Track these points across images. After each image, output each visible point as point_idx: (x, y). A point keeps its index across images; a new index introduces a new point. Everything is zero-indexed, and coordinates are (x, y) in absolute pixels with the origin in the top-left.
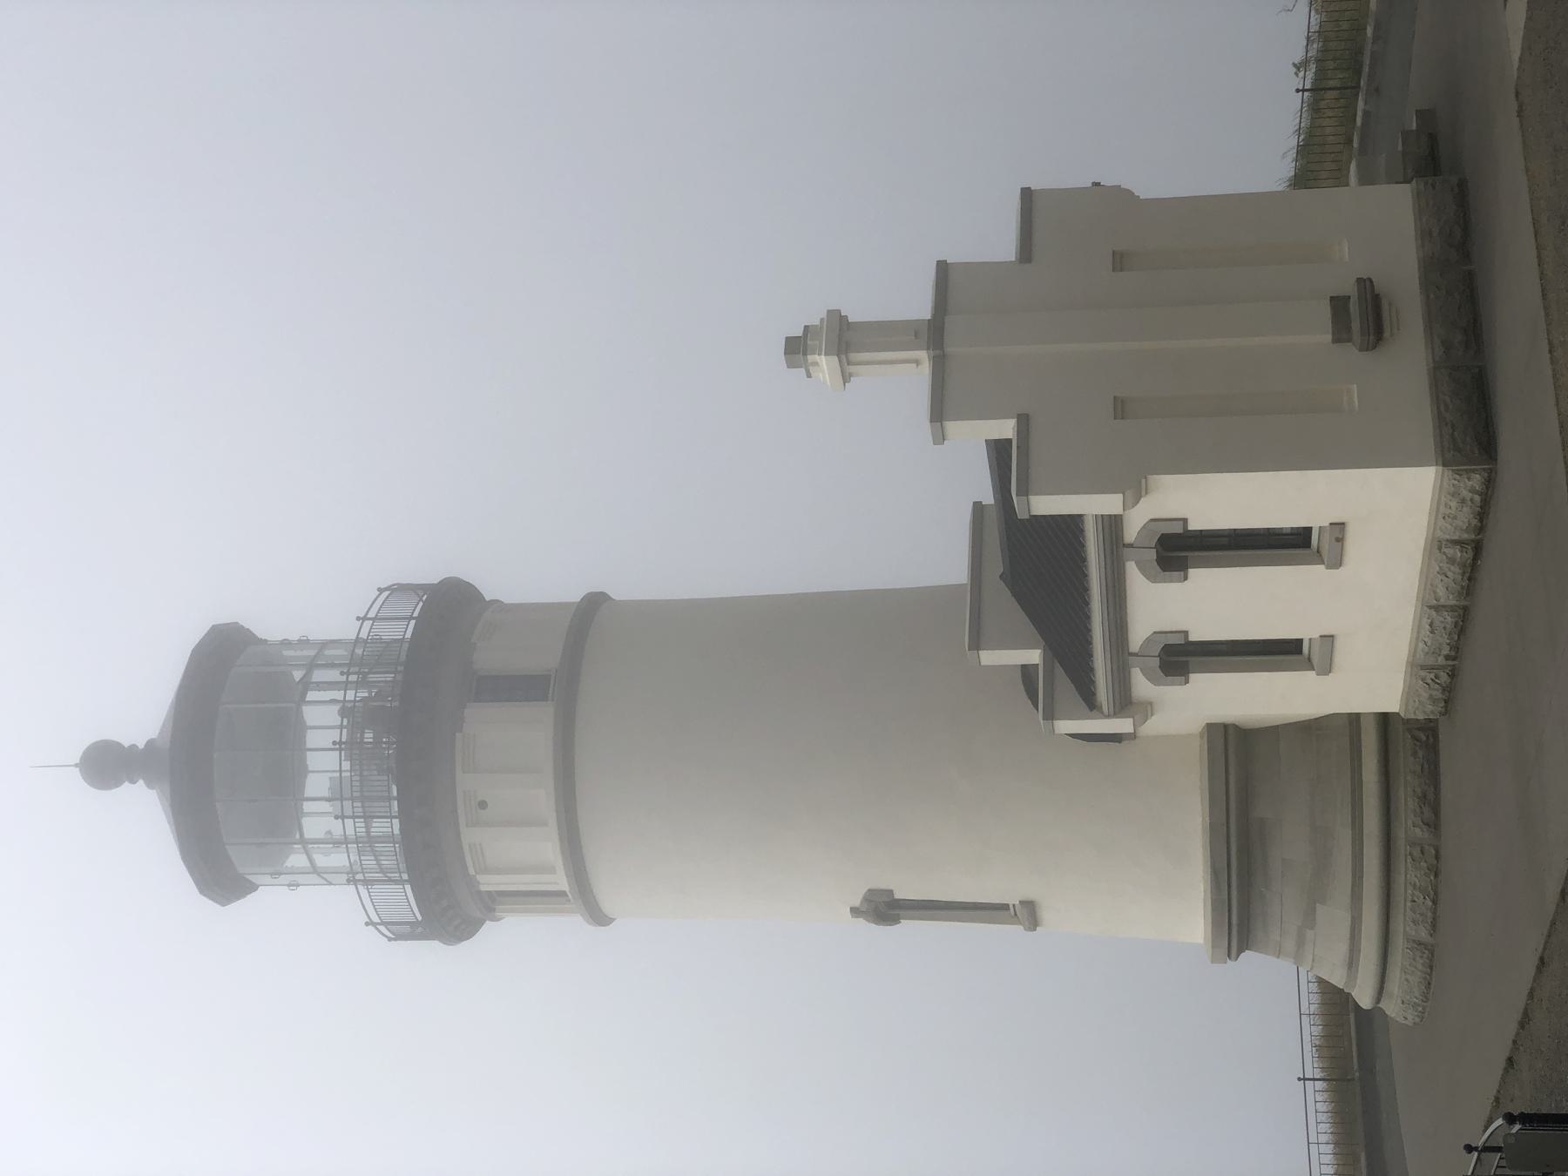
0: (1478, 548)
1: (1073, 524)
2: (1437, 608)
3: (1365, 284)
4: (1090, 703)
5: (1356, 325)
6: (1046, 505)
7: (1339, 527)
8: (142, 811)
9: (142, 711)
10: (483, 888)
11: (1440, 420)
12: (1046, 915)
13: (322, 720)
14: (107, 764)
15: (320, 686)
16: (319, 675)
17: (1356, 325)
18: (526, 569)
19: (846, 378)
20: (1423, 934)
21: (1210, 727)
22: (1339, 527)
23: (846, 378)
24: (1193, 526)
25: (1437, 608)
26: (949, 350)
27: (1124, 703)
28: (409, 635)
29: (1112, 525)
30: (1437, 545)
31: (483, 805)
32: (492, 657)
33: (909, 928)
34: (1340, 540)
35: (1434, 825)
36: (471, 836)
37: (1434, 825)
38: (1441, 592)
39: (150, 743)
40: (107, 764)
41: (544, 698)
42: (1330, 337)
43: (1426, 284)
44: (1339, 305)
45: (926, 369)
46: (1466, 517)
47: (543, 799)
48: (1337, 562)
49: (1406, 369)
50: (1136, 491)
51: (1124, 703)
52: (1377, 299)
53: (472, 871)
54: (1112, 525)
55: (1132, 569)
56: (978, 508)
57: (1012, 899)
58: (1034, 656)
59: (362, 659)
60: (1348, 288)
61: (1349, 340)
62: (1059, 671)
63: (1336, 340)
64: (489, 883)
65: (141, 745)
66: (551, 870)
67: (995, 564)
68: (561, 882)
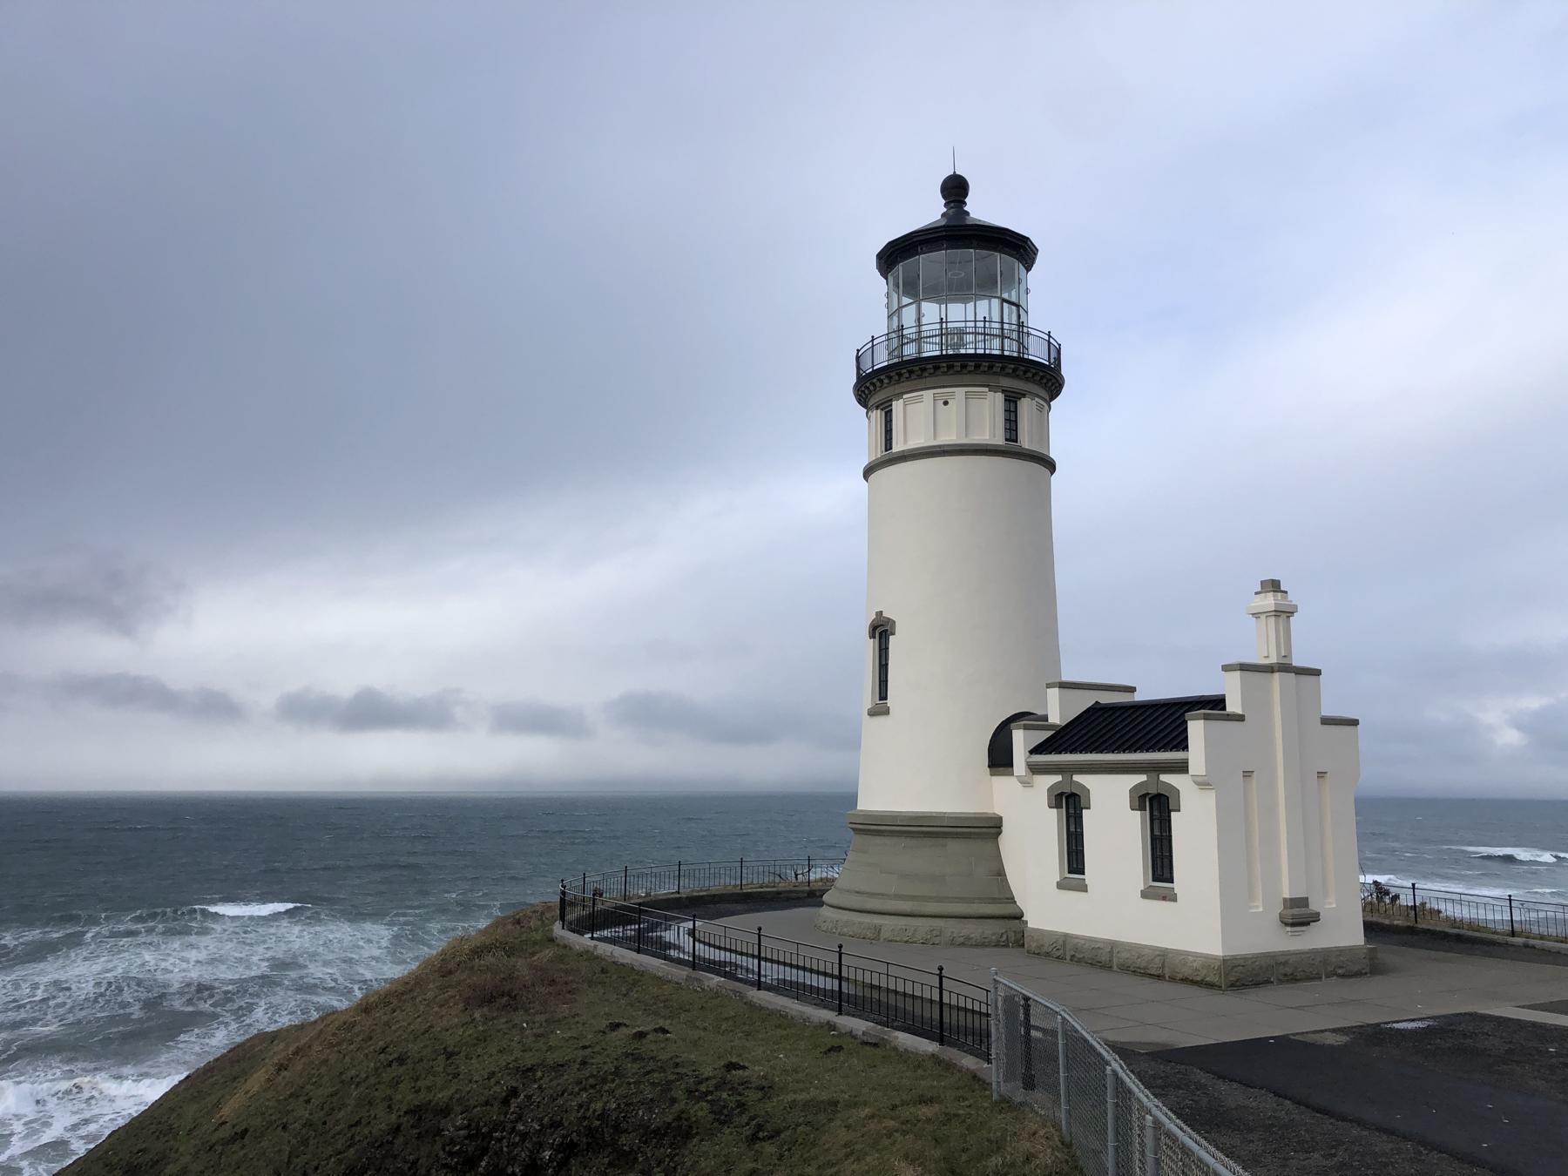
0: (1159, 977)
1: (1183, 744)
2: (1111, 952)
3: (1315, 917)
5: (1296, 911)
6: (1196, 729)
7: (1174, 898)
8: (932, 211)
11: (1245, 958)
13: (986, 308)
14: (955, 189)
17: (1296, 911)
18: (1066, 426)
19: (1256, 615)
20: (883, 935)
21: (1001, 818)
22: (1174, 898)
23: (1256, 615)
24: (1173, 814)
25: (1111, 952)
26: (1277, 675)
27: (1035, 769)
29: (1182, 768)
30: (1164, 953)
31: (946, 403)
32: (1026, 407)
33: (869, 647)
34: (1164, 898)
35: (952, 943)
36: (928, 395)
37: (952, 943)
38: (1125, 955)
40: (955, 189)
42: (1287, 896)
43: (1315, 952)
44: (1303, 902)
45: (1267, 662)
46: (1186, 972)
50: (1203, 784)
52: (1308, 924)
54: (1182, 768)
55: (1143, 778)
56: (1132, 690)
57: (890, 702)
60: (1314, 906)
61: (1285, 908)
62: (1051, 733)
64: (897, 406)
66: (905, 441)
67: (1107, 698)
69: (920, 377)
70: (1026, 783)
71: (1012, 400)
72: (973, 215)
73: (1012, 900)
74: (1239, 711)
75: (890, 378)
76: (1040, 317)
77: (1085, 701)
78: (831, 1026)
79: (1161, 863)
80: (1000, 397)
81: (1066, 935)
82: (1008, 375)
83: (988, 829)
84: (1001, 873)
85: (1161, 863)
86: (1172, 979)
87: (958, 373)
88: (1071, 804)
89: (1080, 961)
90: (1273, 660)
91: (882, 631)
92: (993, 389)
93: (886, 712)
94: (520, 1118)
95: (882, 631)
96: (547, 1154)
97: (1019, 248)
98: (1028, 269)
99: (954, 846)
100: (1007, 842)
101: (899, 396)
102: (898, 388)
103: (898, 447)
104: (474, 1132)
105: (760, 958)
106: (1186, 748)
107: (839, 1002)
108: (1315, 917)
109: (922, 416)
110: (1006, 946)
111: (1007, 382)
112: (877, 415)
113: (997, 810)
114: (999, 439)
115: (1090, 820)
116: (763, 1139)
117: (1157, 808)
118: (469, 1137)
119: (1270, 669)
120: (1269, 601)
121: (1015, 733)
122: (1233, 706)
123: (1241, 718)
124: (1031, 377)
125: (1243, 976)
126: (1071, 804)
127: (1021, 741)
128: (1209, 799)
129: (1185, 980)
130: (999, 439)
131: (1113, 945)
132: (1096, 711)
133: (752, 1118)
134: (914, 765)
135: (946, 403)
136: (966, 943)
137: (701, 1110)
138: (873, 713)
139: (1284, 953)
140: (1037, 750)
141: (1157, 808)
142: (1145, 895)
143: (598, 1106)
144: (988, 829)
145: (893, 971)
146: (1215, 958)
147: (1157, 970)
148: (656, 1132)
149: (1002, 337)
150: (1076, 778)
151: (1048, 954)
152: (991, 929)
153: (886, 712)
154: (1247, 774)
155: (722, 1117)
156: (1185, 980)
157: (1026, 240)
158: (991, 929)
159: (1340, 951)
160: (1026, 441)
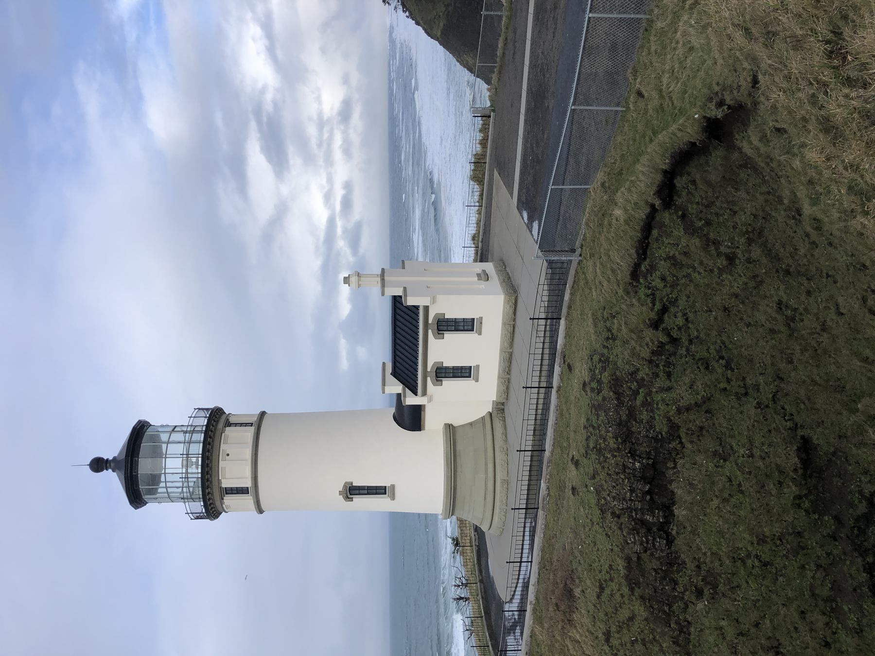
0: (514, 327)
1: (417, 308)
6: (411, 301)
9: (113, 449)
10: (224, 486)
14: (98, 465)
19: (359, 286)
20: (505, 478)
26: (386, 278)
27: (424, 393)
30: (504, 324)
31: (228, 455)
35: (506, 440)
36: (222, 464)
37: (506, 440)
39: (115, 458)
40: (98, 465)
43: (498, 274)
44: (479, 275)
46: (511, 312)
49: (495, 281)
50: (434, 301)
54: (426, 309)
55: (430, 332)
56: (384, 364)
57: (387, 484)
64: (225, 484)
65: (111, 458)
69: (211, 469)
70: (430, 400)
71: (228, 424)
72: (116, 455)
73: (483, 418)
75: (208, 487)
76: (182, 420)
77: (390, 379)
78: (559, 388)
79: (466, 325)
80: (227, 428)
81: (499, 377)
82: (217, 425)
83: (450, 429)
84: (471, 424)
85: (466, 325)
86: (514, 320)
87: (212, 448)
88: (442, 373)
89: (510, 370)
90: (379, 279)
91: (352, 491)
92: (223, 431)
93: (393, 486)
94: (624, 499)
95: (352, 491)
96: (637, 465)
99: (459, 447)
100: (456, 423)
101: (219, 482)
102: (215, 483)
103: (248, 483)
104: (634, 530)
105: (521, 562)
107: (549, 387)
108: (484, 271)
109: (233, 471)
111: (221, 425)
112: (229, 500)
113: (440, 428)
114: (251, 430)
115: (450, 362)
116: (612, 335)
117: (445, 326)
118: (638, 533)
119: (383, 280)
120: (354, 279)
121: (407, 403)
122: (399, 292)
123: (405, 289)
124: (216, 421)
125: (511, 289)
126: (442, 373)
127: (411, 400)
128: (440, 298)
129: (515, 313)
131: (502, 351)
132: (394, 374)
133: (604, 347)
134: (417, 474)
135: (228, 455)
137: (606, 376)
138: (393, 498)
139: (499, 279)
140: (415, 393)
141: (445, 326)
142: (480, 334)
143: (612, 443)
144: (450, 429)
145: (542, 282)
146: (505, 298)
148: (618, 399)
149: (190, 442)
150: (429, 369)
151: (508, 388)
152: (498, 425)
153: (393, 486)
155: (605, 361)
156: (515, 313)
157: (140, 422)
158: (498, 425)
159: (496, 267)
160: (254, 420)
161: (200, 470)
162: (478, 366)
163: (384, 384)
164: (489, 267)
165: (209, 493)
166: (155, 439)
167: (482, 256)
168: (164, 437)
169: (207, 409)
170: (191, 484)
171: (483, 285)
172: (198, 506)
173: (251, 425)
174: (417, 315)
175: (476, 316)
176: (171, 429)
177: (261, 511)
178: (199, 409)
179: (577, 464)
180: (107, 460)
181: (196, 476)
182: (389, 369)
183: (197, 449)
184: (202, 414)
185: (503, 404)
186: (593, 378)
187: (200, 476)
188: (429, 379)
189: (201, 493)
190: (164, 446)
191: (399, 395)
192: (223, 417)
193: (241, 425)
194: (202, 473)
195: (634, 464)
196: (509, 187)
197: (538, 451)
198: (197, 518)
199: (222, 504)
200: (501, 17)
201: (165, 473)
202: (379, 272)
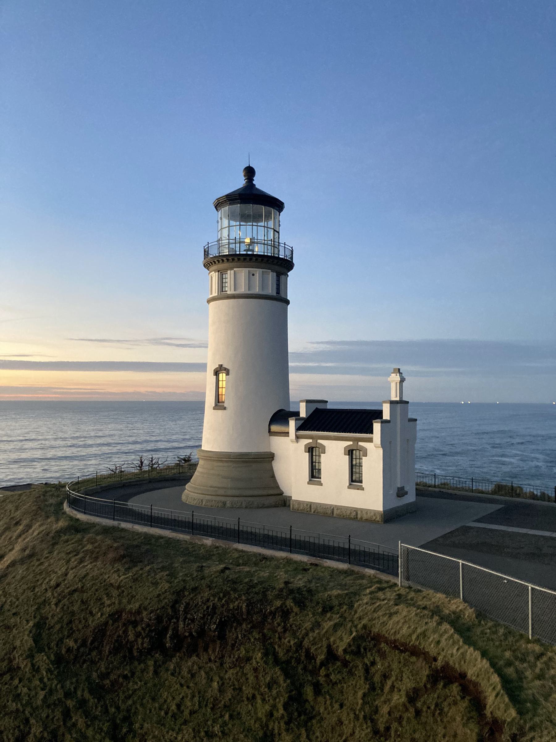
1: (371, 432)
3: (406, 493)
4: (298, 429)
6: (377, 427)
12: (220, 412)
14: (250, 172)
15: (268, 231)
16: (271, 232)
25: (333, 509)
26: (399, 405)
28: (280, 256)
30: (356, 510)
31: (253, 275)
37: (258, 507)
39: (255, 185)
40: (250, 172)
41: (277, 293)
47: (257, 290)
48: (349, 488)
51: (298, 437)
53: (235, 269)
54: (370, 440)
56: (327, 402)
58: (303, 414)
59: (275, 245)
60: (406, 489)
62: (303, 421)
63: (398, 488)
65: (254, 182)
68: (229, 290)
71: (278, 276)
72: (257, 186)
73: (278, 487)
74: (389, 419)
80: (275, 274)
82: (278, 265)
84: (273, 476)
92: (273, 271)
97: (277, 205)
98: (280, 213)
106: (372, 433)
108: (406, 493)
110: (278, 507)
111: (277, 268)
114: (275, 294)
122: (386, 416)
130: (275, 294)
132: (317, 410)
136: (263, 507)
138: (214, 408)
139: (398, 507)
147: (353, 517)
152: (272, 500)
154: (390, 443)
157: (283, 204)
161: (241, 253)
162: (321, 485)
163: (308, 402)
164: (411, 498)
165: (223, 261)
166: (268, 217)
167: (423, 491)
168: (271, 224)
169: (292, 258)
170: (231, 246)
171: (393, 492)
172: (214, 252)
173: (278, 293)
174: (366, 432)
175: (364, 485)
176: (277, 230)
177: (209, 301)
178: (292, 251)
179: (223, 571)
180: (254, 180)
181: (237, 249)
182: (321, 406)
183: (258, 250)
184: (288, 253)
185: (289, 506)
186: (291, 591)
187: (238, 253)
188: (311, 441)
189: (225, 254)
190: (262, 224)
191: (297, 414)
192: (285, 270)
193: (278, 285)
194: (240, 255)
195: (215, 623)
196: (490, 518)
197: (239, 535)
198: (205, 251)
199: (215, 271)
200: (408, 552)
201: (240, 225)
202: (404, 399)
